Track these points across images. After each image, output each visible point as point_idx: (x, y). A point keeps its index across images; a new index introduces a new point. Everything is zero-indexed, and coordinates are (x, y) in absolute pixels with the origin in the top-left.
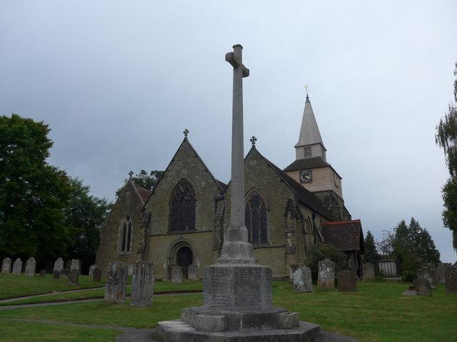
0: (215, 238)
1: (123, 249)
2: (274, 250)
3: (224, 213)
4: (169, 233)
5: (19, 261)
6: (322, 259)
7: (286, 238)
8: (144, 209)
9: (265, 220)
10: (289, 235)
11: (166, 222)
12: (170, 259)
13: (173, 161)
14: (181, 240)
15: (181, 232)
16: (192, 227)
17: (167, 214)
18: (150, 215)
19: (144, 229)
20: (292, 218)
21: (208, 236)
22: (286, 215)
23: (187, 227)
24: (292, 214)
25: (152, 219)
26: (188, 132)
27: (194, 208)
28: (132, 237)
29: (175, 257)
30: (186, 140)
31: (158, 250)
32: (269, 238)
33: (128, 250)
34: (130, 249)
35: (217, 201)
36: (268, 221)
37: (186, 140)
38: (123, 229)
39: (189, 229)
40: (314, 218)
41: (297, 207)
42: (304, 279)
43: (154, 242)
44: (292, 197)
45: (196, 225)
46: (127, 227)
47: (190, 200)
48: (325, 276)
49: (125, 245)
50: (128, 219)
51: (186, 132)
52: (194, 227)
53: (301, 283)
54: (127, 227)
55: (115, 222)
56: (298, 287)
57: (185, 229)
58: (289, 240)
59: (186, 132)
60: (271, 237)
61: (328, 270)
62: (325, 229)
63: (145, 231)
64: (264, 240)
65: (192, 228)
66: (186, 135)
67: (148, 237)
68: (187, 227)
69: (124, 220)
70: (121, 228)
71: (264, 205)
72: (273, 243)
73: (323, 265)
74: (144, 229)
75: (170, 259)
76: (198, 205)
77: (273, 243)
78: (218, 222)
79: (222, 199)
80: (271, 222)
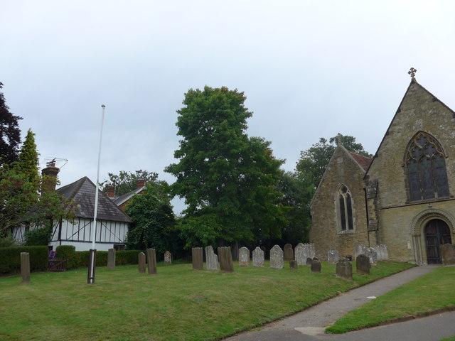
1: (344, 228)
4: (408, 203)
5: (276, 251)
8: (366, 177)
12: (416, 236)
13: (399, 111)
14: (430, 211)
15: (426, 201)
17: (403, 179)
18: (377, 184)
19: (373, 200)
23: (436, 194)
25: (380, 188)
26: (415, 71)
27: (443, 167)
28: (354, 211)
30: (413, 82)
31: (395, 225)
33: (351, 227)
34: (354, 227)
37: (413, 82)
38: (339, 201)
39: (440, 195)
43: (387, 216)
47: (433, 158)
49: (347, 221)
50: (344, 190)
51: (412, 72)
52: (446, 193)
55: (328, 196)
59: (412, 72)
63: (375, 203)
65: (445, 194)
66: (413, 75)
68: (436, 194)
69: (339, 193)
70: (337, 202)
74: (373, 200)
75: (416, 236)
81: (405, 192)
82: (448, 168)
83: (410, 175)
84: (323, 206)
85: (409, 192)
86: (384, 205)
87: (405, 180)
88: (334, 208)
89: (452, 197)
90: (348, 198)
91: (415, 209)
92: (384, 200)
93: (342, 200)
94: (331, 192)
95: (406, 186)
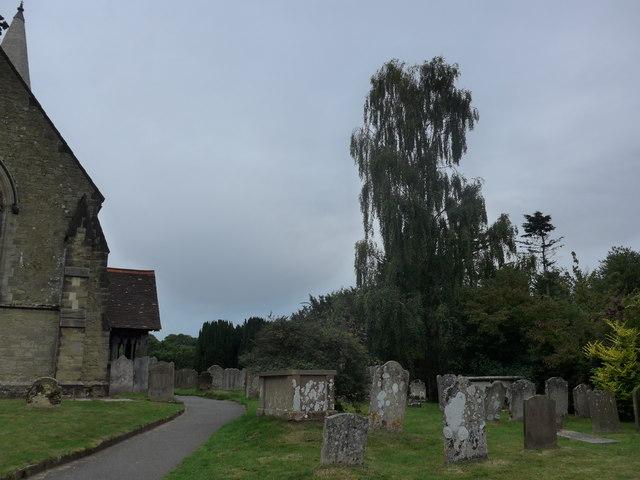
2: (18, 314)
7: (65, 289)
10: (76, 282)
42: (469, 422)
48: (388, 403)
56: (456, 445)
58: (72, 296)
60: (11, 282)
61: (395, 387)
72: (17, 297)
73: (386, 376)
77: (17, 297)
80: (16, 242)
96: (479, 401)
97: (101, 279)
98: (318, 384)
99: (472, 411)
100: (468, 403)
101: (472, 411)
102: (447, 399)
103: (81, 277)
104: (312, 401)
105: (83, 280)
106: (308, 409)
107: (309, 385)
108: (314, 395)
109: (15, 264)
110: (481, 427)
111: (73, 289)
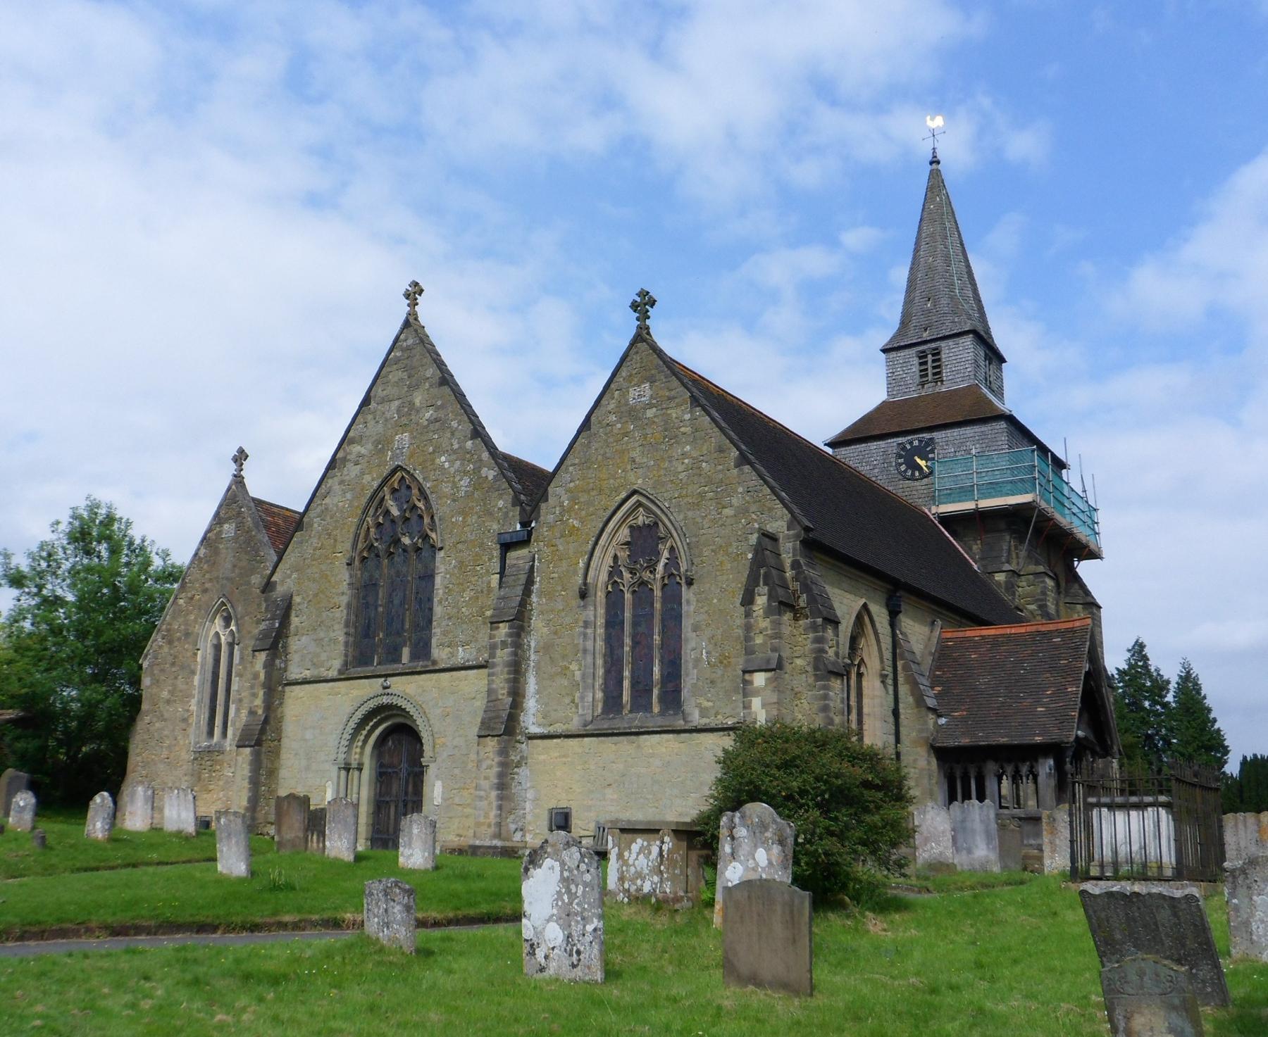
0: (490, 692)
3: (527, 592)
4: (344, 676)
6: (755, 795)
9: (678, 617)
11: (339, 634)
14: (385, 700)
15: (382, 669)
16: (422, 650)
17: (344, 600)
20: (768, 612)
21: (474, 682)
22: (748, 600)
23: (406, 652)
24: (771, 597)
25: (295, 620)
27: (428, 577)
28: (234, 687)
29: (367, 761)
32: (685, 693)
35: (506, 547)
36: (687, 624)
38: (210, 651)
39: (414, 657)
40: (894, 614)
41: (796, 565)
42: (566, 917)
44: (779, 523)
45: (434, 641)
46: (224, 648)
50: (227, 621)
53: (554, 934)
54: (224, 648)
55: (187, 635)
56: (540, 954)
57: (397, 659)
58: (756, 703)
61: (761, 856)
62: (944, 655)
63: (269, 665)
64: (672, 699)
65: (424, 663)
67: (275, 686)
68: (406, 652)
69: (218, 624)
70: (204, 654)
71: (673, 560)
72: (704, 712)
73: (741, 832)
74: (262, 657)
76: (444, 567)
77: (704, 712)
78: (504, 629)
79: (525, 542)
81: (342, 639)
82: (438, 580)
83: (365, 591)
84: (173, 664)
85: (351, 639)
86: (295, 672)
87: (349, 605)
88: (193, 673)
89: (434, 662)
90: (231, 646)
91: (355, 693)
92: (295, 658)
93: (217, 648)
94: (195, 621)
95: (347, 625)
96: (588, 877)
97: (816, 668)
98: (649, 845)
99: (572, 896)
100: (565, 881)
101: (572, 896)
102: (527, 870)
103: (766, 671)
104: (639, 875)
105: (769, 674)
106: (633, 888)
107: (635, 847)
108: (642, 863)
109: (697, 661)
110: (590, 928)
111: (756, 693)
